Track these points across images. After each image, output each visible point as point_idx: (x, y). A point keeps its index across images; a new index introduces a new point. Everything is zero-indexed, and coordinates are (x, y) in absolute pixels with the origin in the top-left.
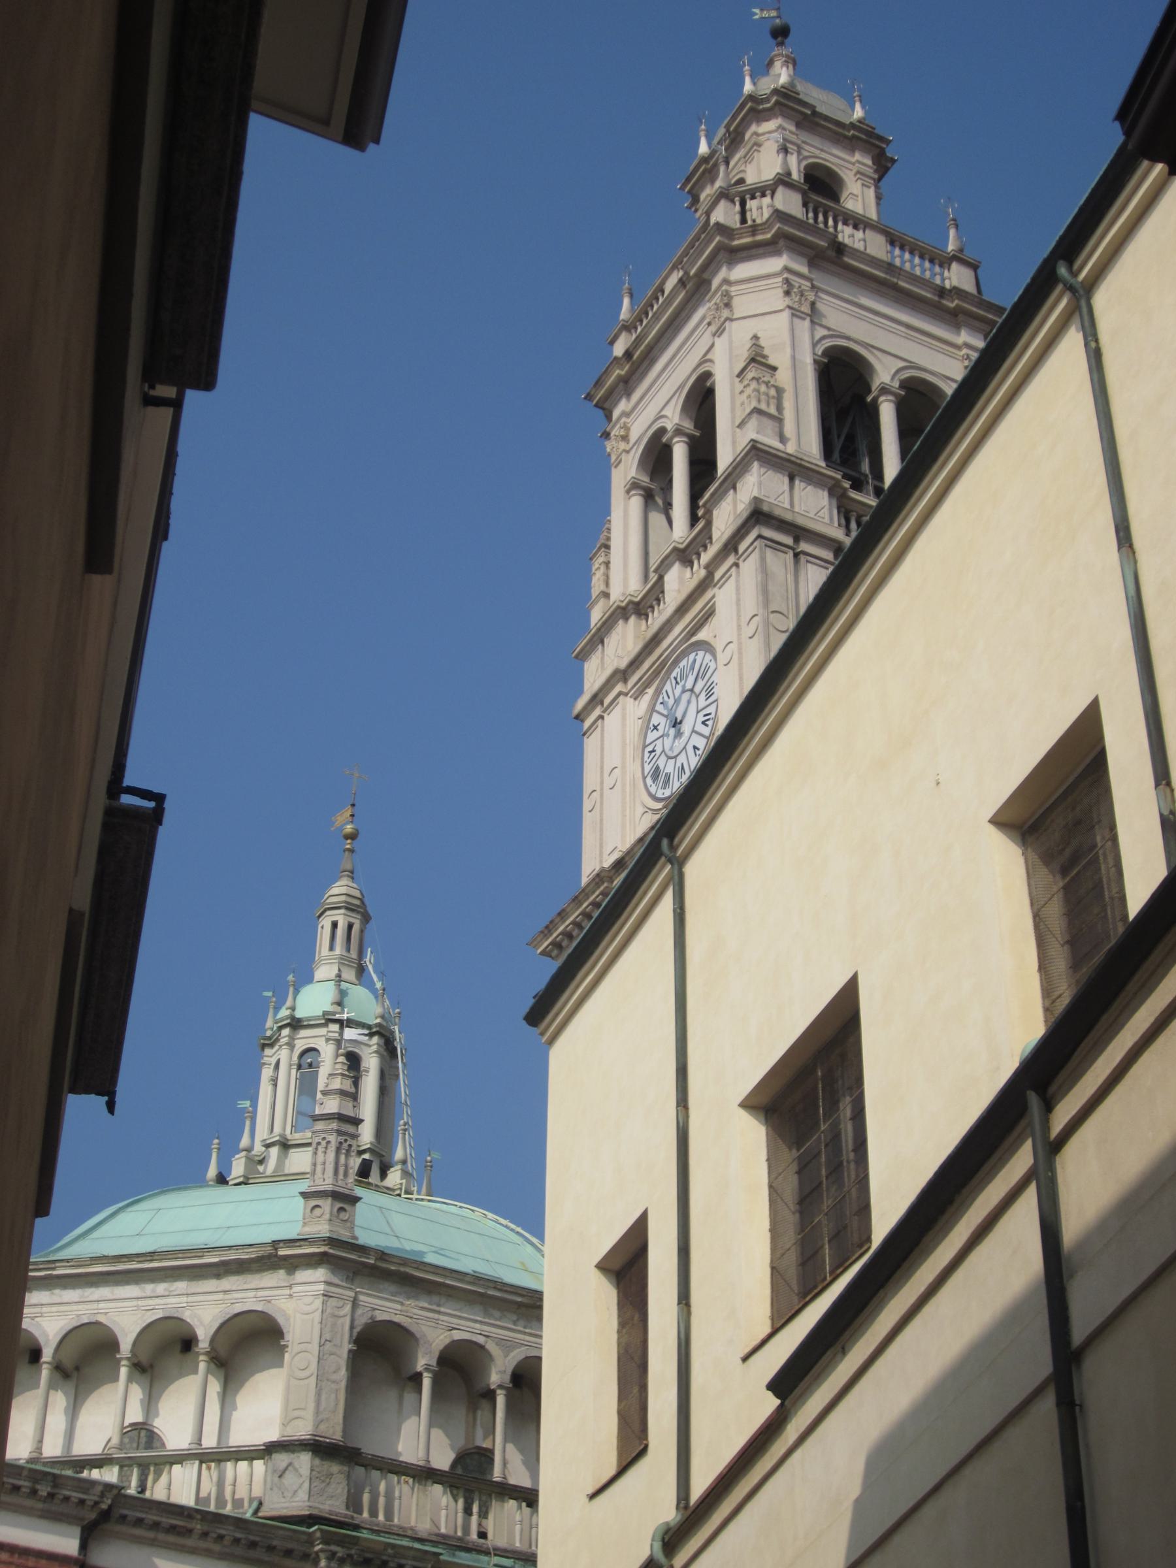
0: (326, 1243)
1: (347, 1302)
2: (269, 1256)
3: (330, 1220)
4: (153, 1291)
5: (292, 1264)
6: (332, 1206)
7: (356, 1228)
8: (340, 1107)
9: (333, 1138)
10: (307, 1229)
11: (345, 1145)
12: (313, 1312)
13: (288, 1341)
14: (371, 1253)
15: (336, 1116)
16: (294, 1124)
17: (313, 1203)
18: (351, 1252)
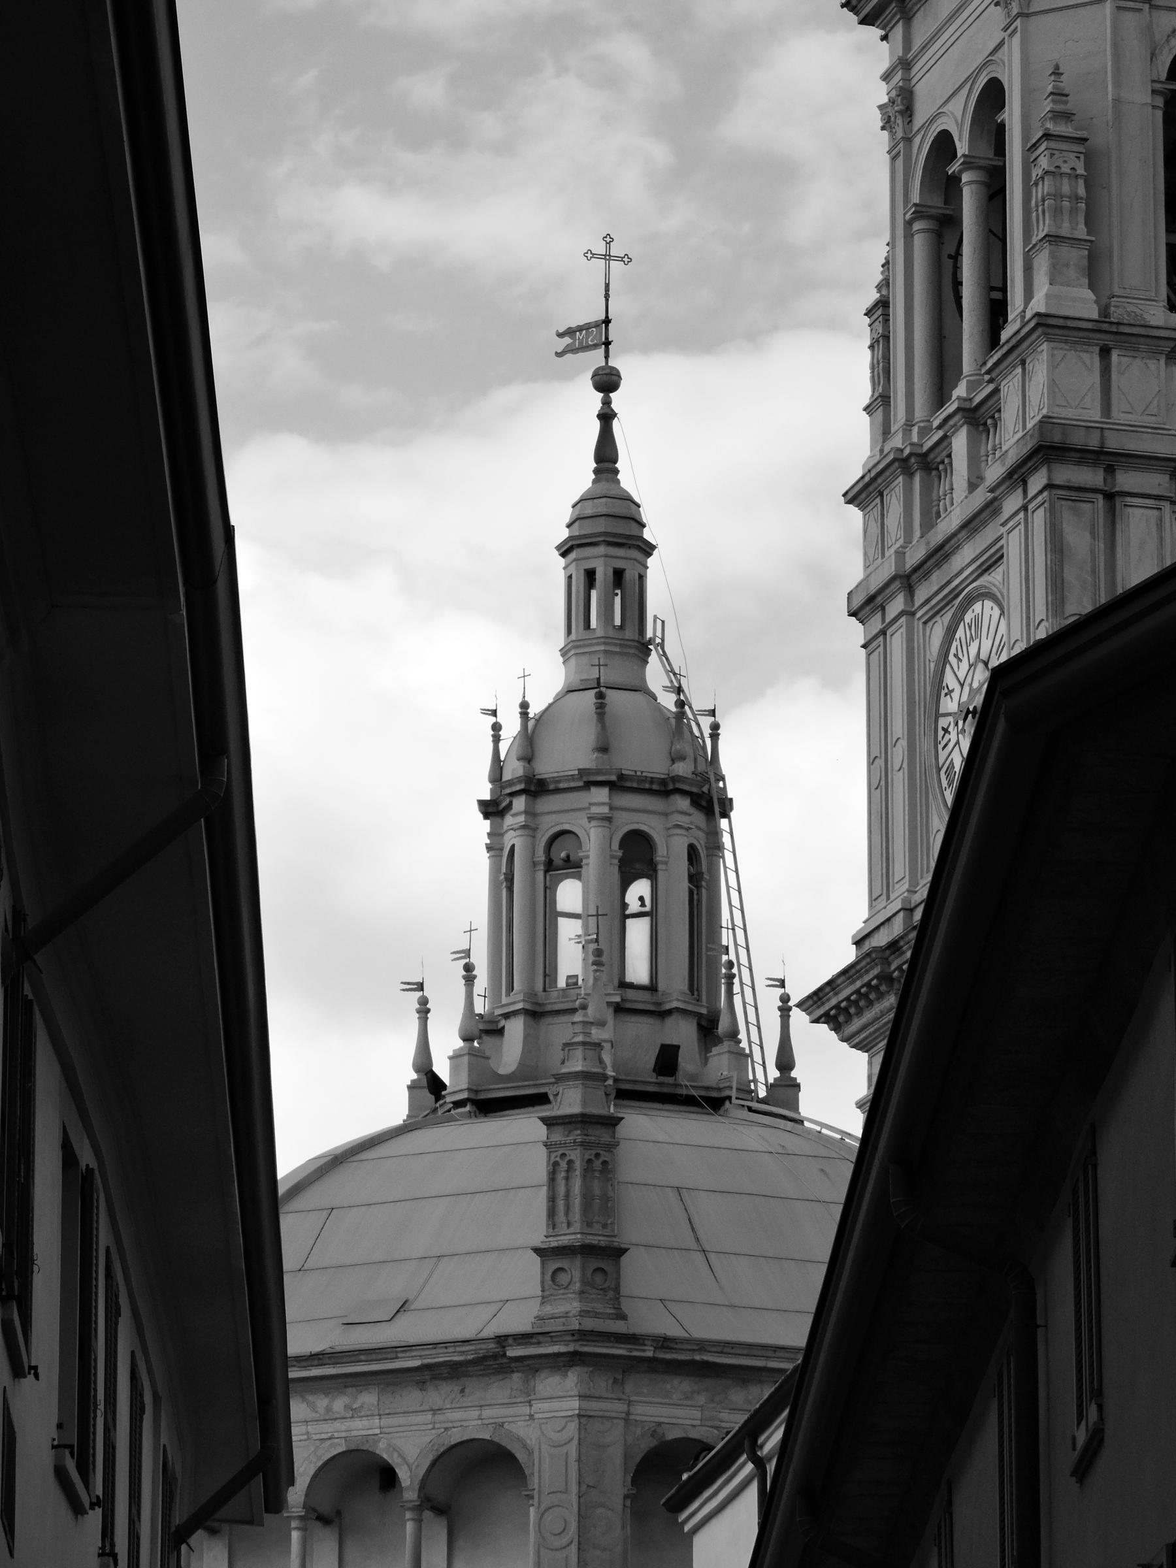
0: (575, 1338)
1: (615, 1421)
2: (495, 1356)
3: (582, 1292)
4: (328, 1409)
5: (533, 1366)
6: (583, 1269)
7: (622, 1299)
8: (584, 1103)
9: (575, 1155)
10: (548, 1309)
11: (597, 1164)
12: (565, 1444)
13: (534, 1489)
14: (646, 1342)
15: (580, 1119)
16: (547, 972)
17: (553, 1265)
18: (616, 1345)
